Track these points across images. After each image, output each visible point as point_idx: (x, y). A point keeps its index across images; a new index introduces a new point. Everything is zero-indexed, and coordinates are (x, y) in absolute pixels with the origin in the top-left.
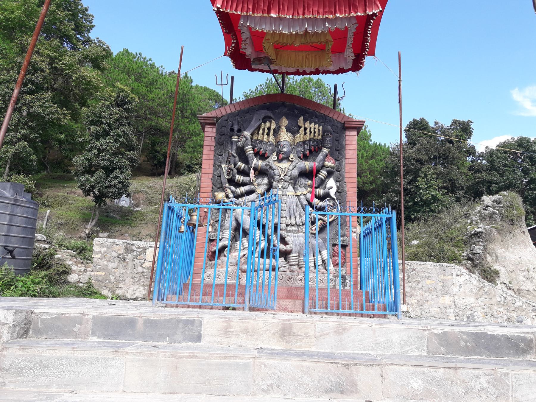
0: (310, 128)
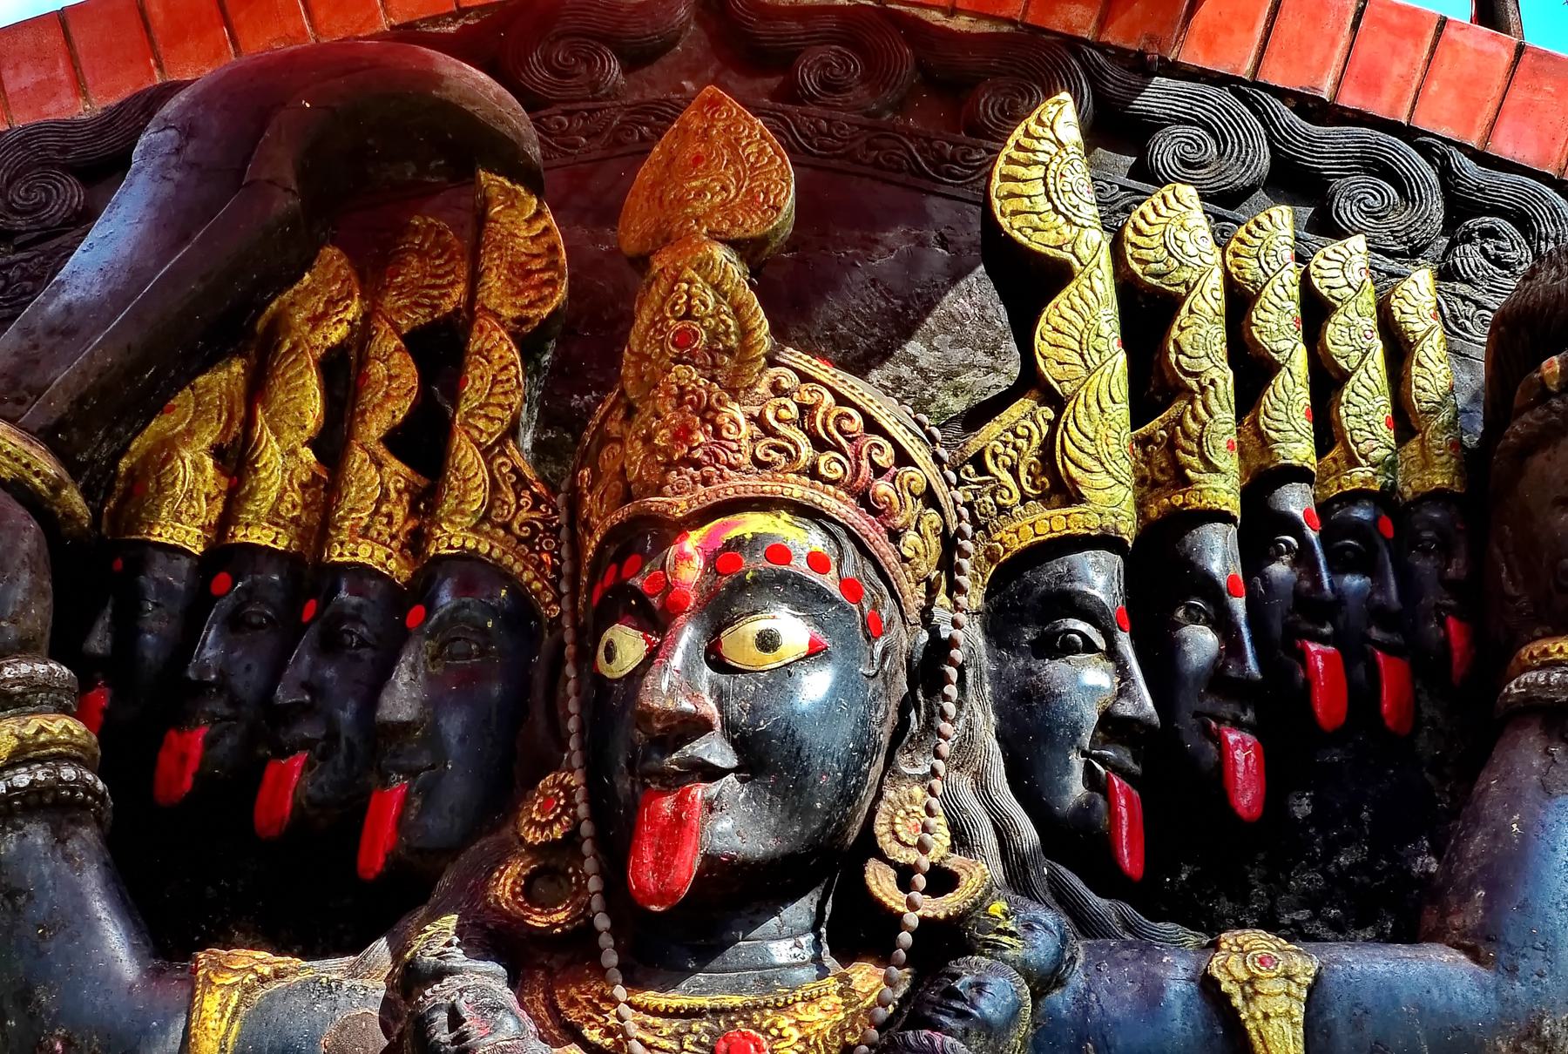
0: (1240, 301)
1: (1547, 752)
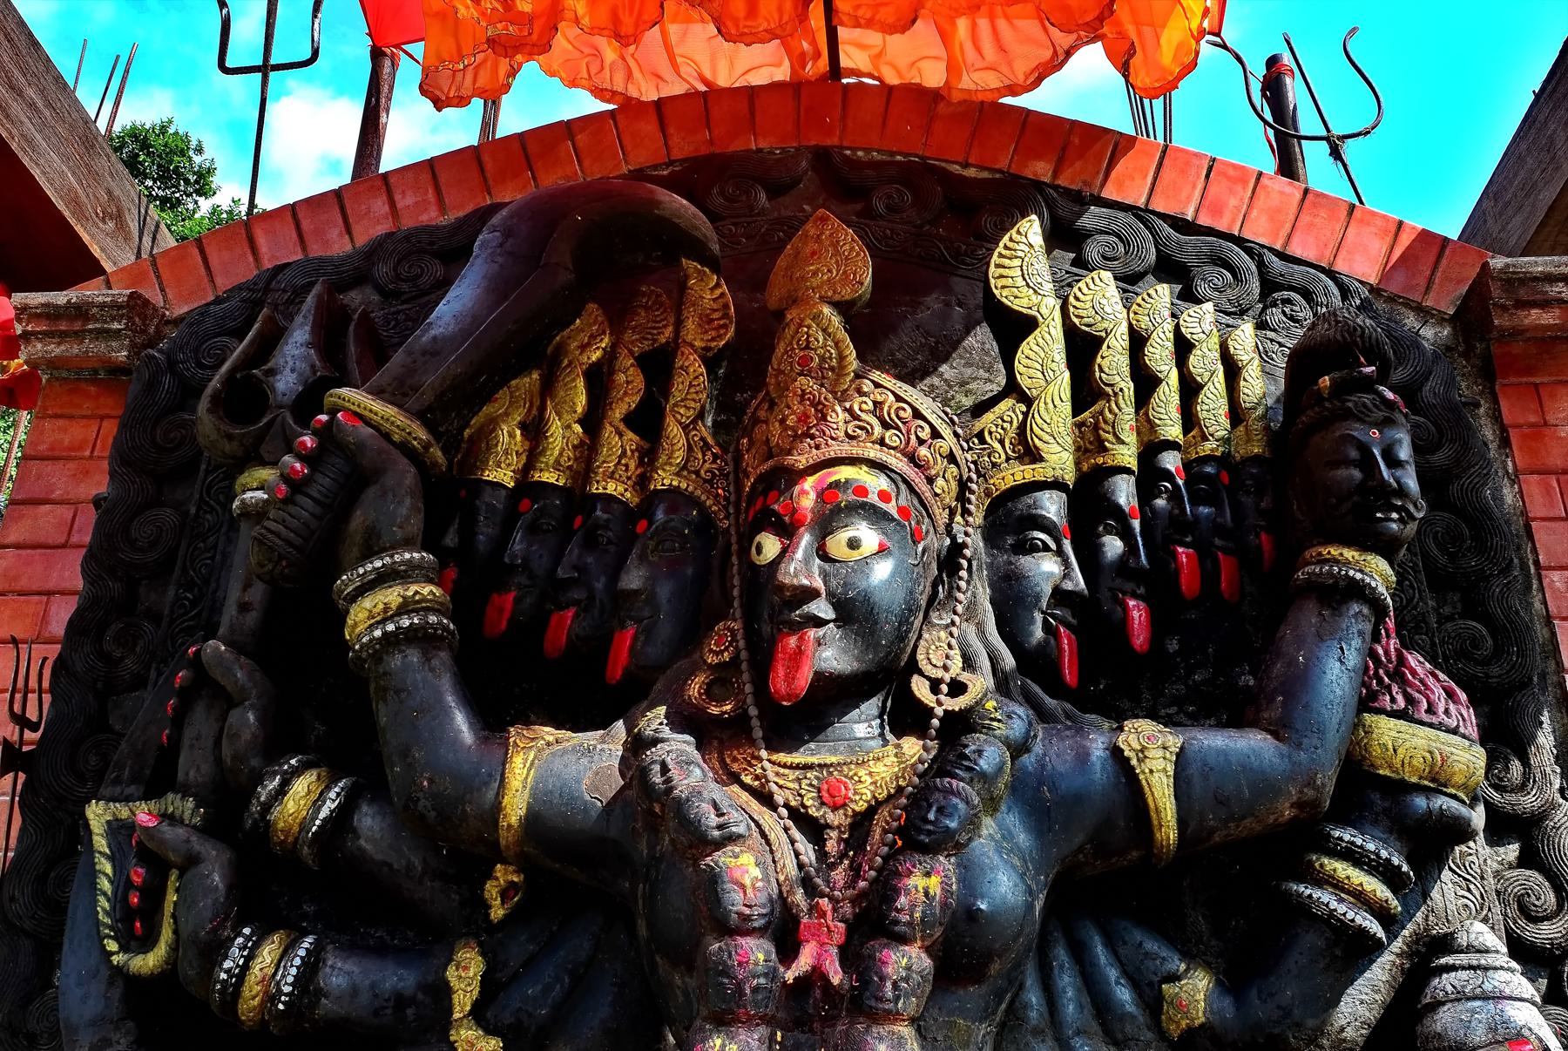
0: (1138, 341)
1: (1320, 614)
